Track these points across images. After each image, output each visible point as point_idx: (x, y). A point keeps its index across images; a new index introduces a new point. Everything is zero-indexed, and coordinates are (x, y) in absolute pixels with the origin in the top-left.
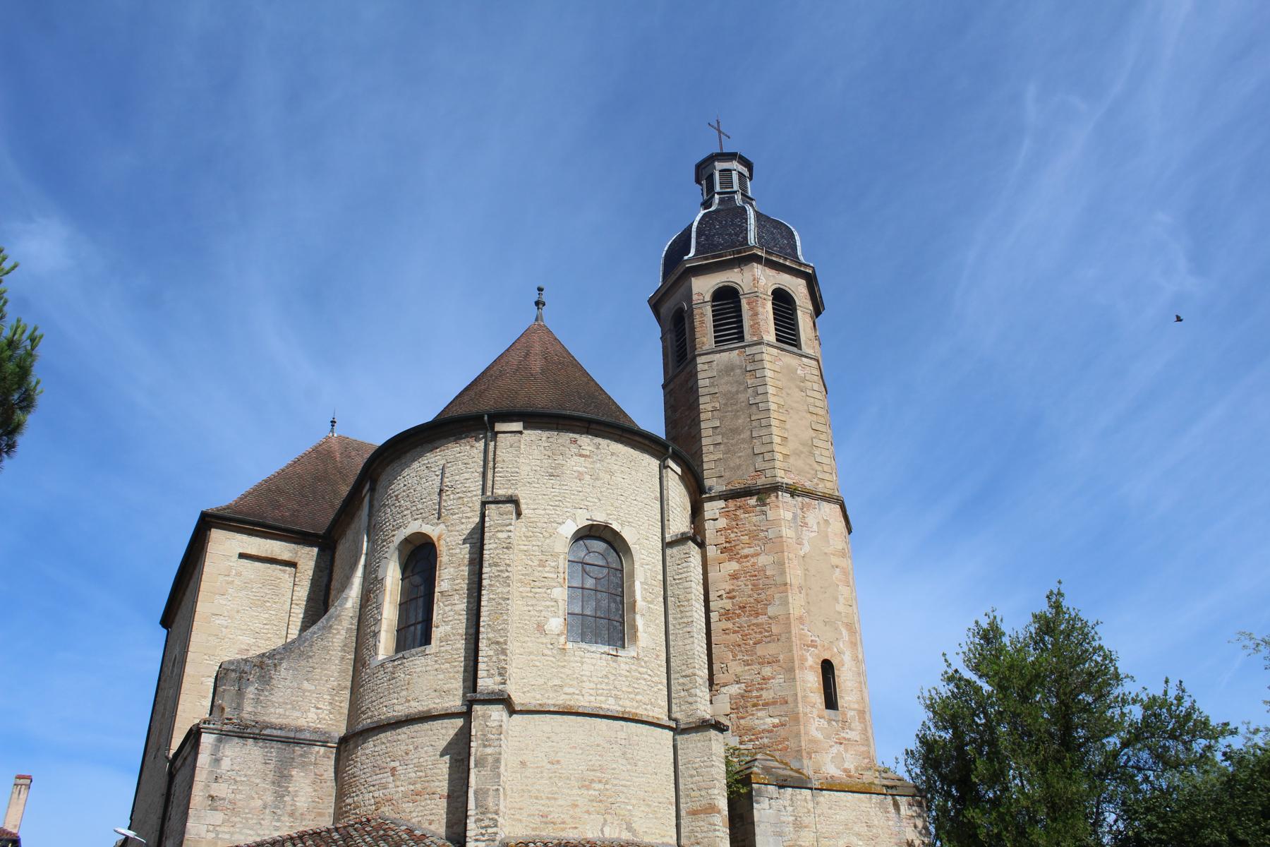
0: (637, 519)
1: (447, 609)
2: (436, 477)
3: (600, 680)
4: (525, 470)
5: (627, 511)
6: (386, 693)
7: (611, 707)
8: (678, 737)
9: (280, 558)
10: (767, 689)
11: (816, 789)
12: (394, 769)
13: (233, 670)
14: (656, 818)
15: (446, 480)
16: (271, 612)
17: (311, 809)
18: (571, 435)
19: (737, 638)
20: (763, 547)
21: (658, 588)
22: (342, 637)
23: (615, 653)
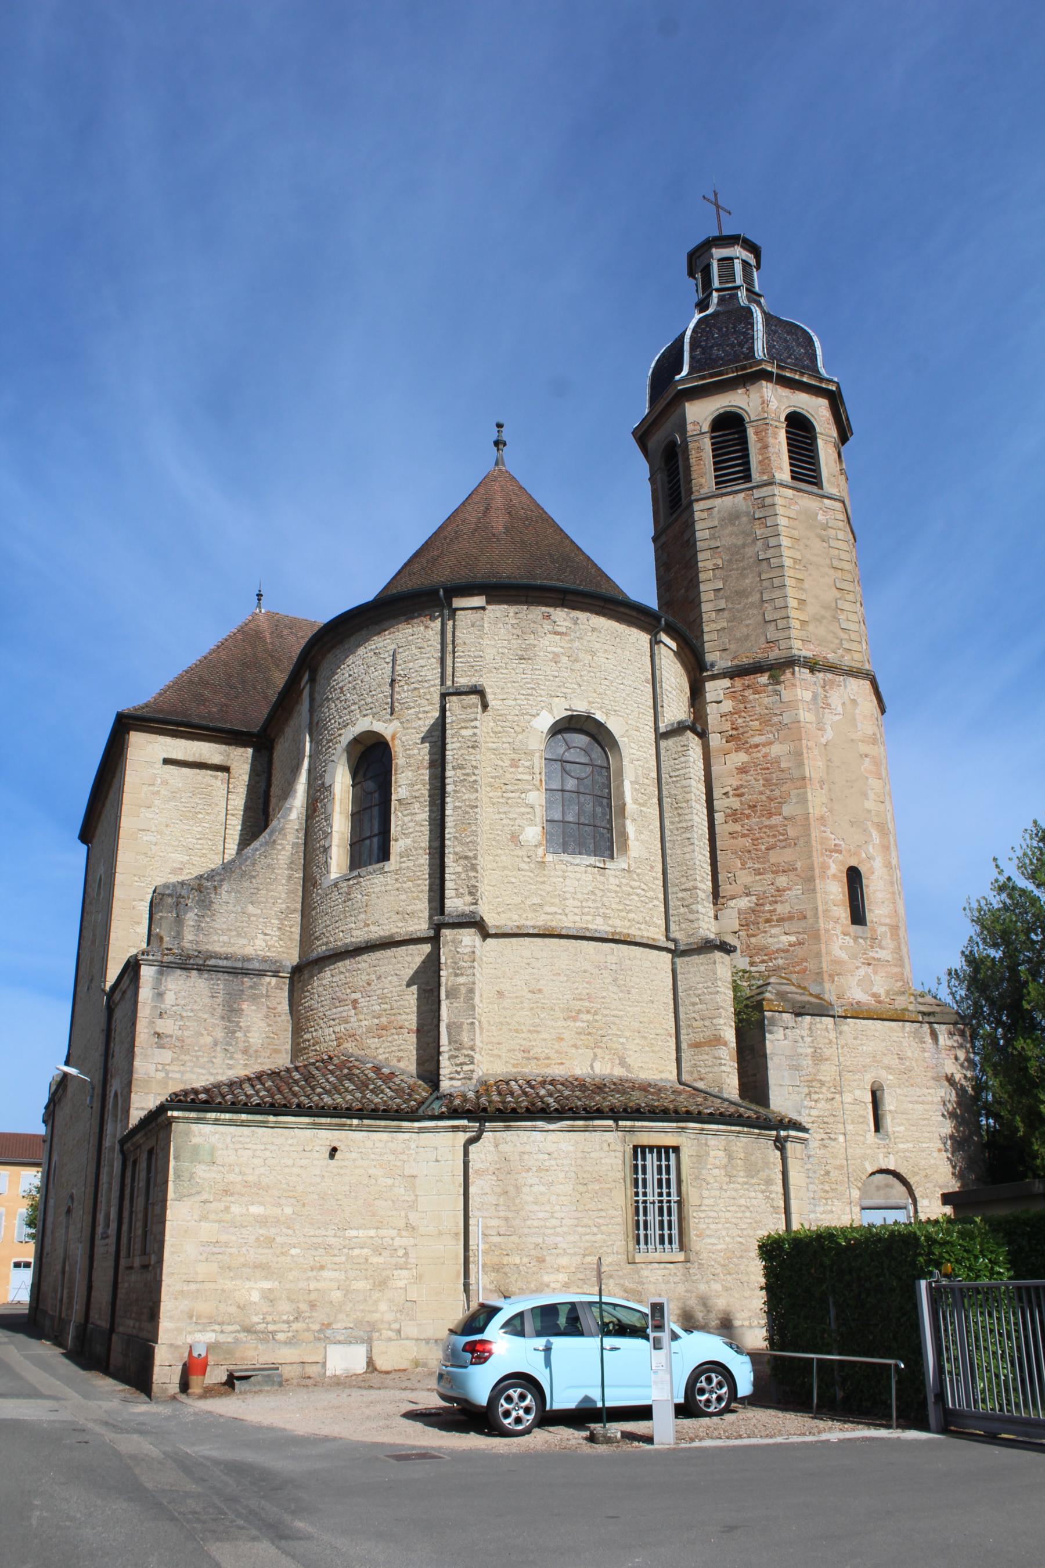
1: (406, 819)
2: (385, 665)
3: (586, 896)
4: (490, 653)
5: (612, 698)
6: (342, 917)
7: (600, 928)
8: (678, 960)
9: (210, 762)
10: (782, 902)
11: (839, 1017)
12: (355, 1002)
13: (169, 895)
14: (653, 1051)
15: (398, 668)
16: (204, 824)
17: (265, 1046)
18: (544, 609)
19: (747, 842)
20: (776, 734)
21: (652, 788)
22: (288, 854)
23: (602, 866)
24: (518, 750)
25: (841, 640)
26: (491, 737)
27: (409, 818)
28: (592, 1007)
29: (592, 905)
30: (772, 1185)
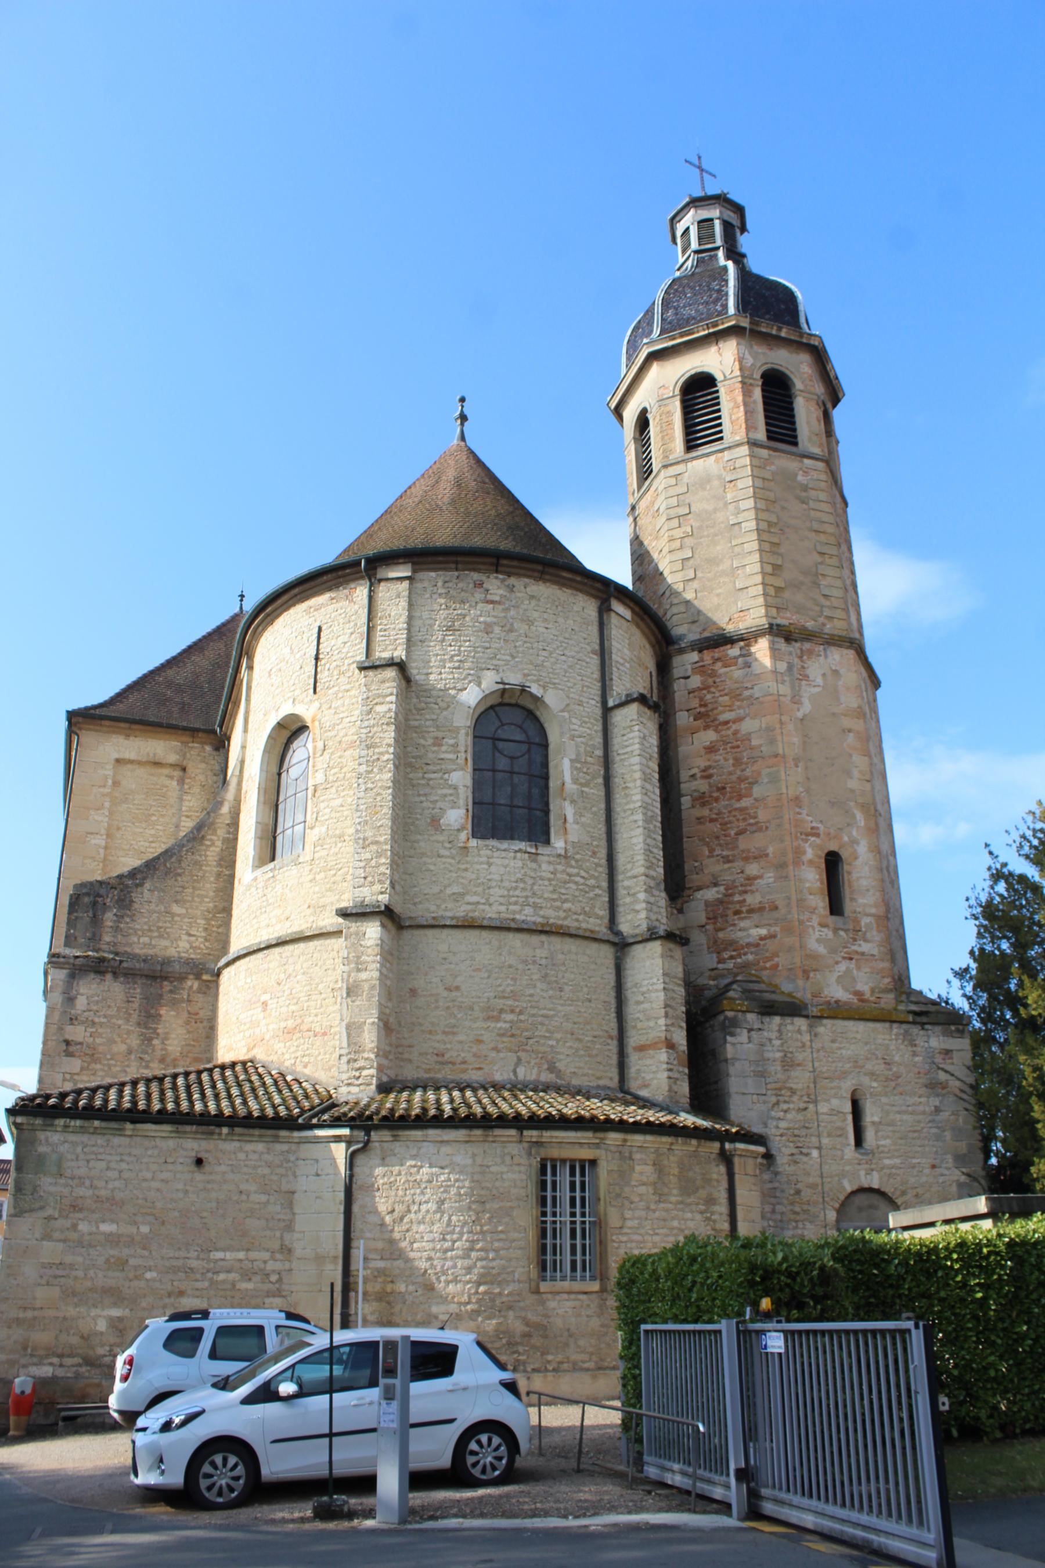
3: (514, 885)
10: (753, 892)
11: (813, 1017)
12: (265, 1004)
14: (590, 1056)
21: (596, 767)
22: (218, 849)
23: (533, 851)
25: (822, 606)
27: (326, 804)
30: (714, 1204)
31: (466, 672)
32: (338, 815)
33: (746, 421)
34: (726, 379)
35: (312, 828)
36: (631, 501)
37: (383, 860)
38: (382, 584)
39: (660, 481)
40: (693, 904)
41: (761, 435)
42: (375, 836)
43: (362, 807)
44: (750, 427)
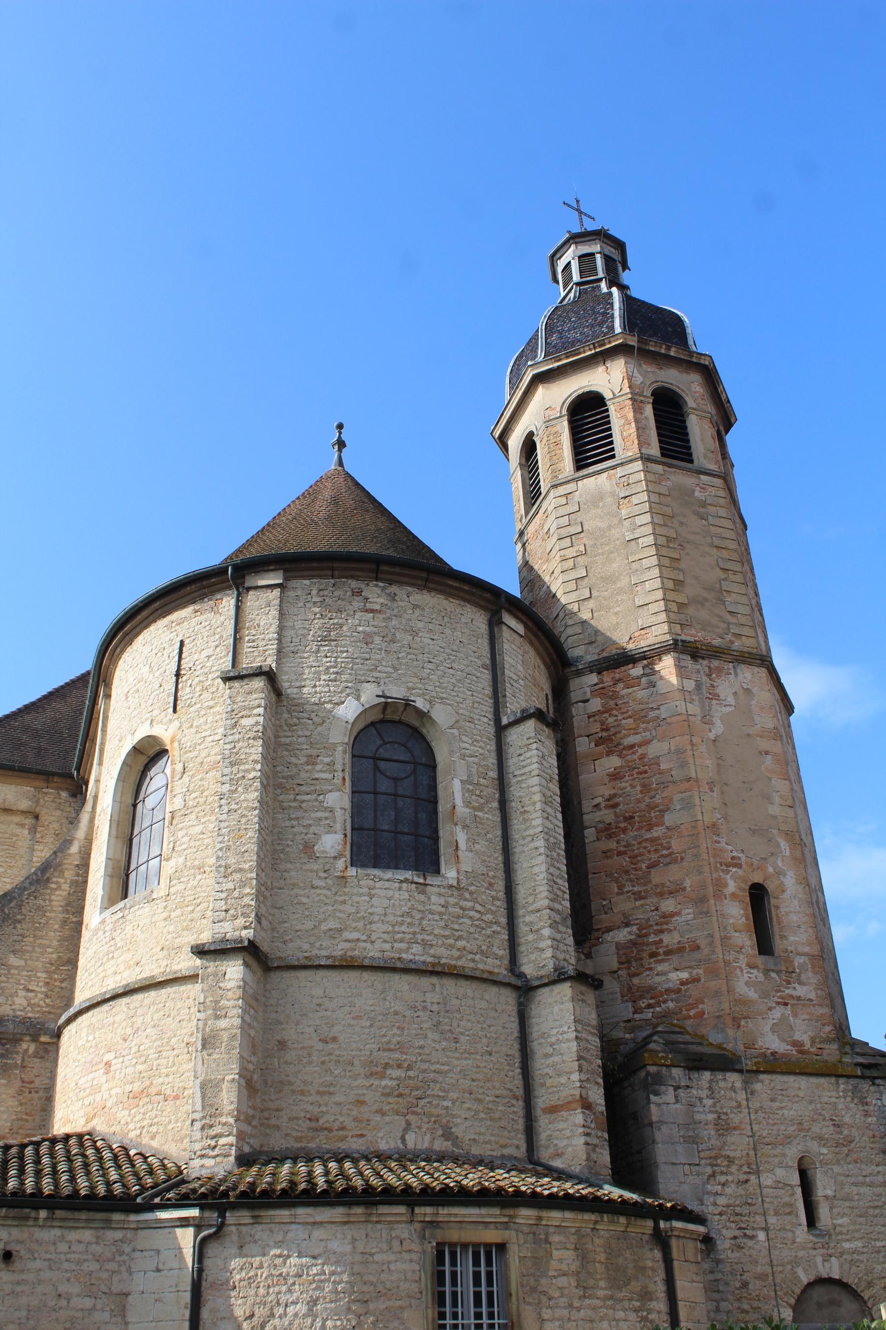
0: (454, 694)
3: (400, 919)
10: (670, 931)
11: (748, 1071)
12: (108, 1064)
14: (491, 1119)
17: (15, 1130)
21: (490, 790)
23: (421, 881)
24: (316, 744)
25: (729, 623)
26: (285, 731)
27: (184, 832)
28: (405, 1060)
29: (407, 930)
31: (344, 684)
32: (197, 843)
33: (639, 437)
34: (615, 397)
35: (168, 860)
36: (519, 526)
37: (247, 890)
38: (251, 593)
39: (550, 503)
40: (602, 948)
41: (654, 450)
42: (238, 862)
43: (224, 830)
44: (642, 443)
